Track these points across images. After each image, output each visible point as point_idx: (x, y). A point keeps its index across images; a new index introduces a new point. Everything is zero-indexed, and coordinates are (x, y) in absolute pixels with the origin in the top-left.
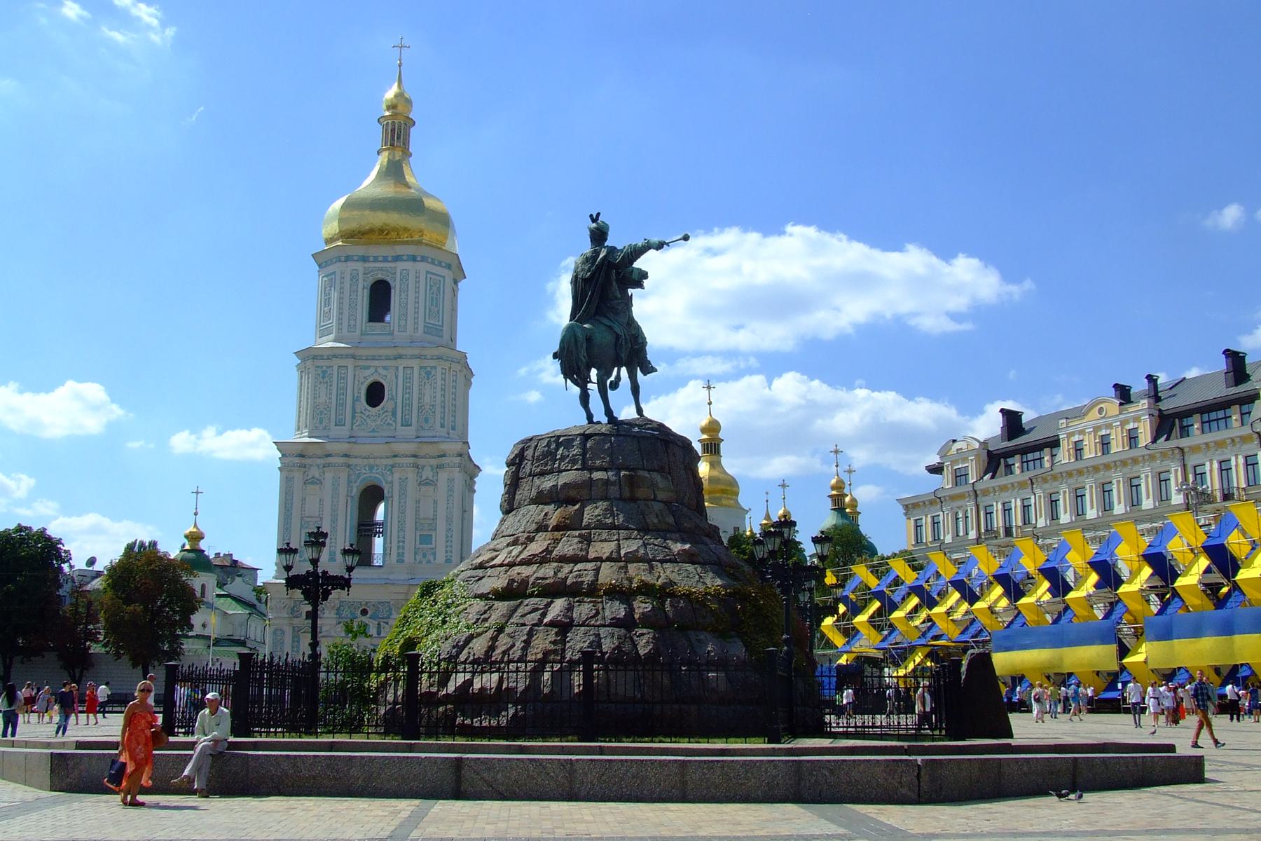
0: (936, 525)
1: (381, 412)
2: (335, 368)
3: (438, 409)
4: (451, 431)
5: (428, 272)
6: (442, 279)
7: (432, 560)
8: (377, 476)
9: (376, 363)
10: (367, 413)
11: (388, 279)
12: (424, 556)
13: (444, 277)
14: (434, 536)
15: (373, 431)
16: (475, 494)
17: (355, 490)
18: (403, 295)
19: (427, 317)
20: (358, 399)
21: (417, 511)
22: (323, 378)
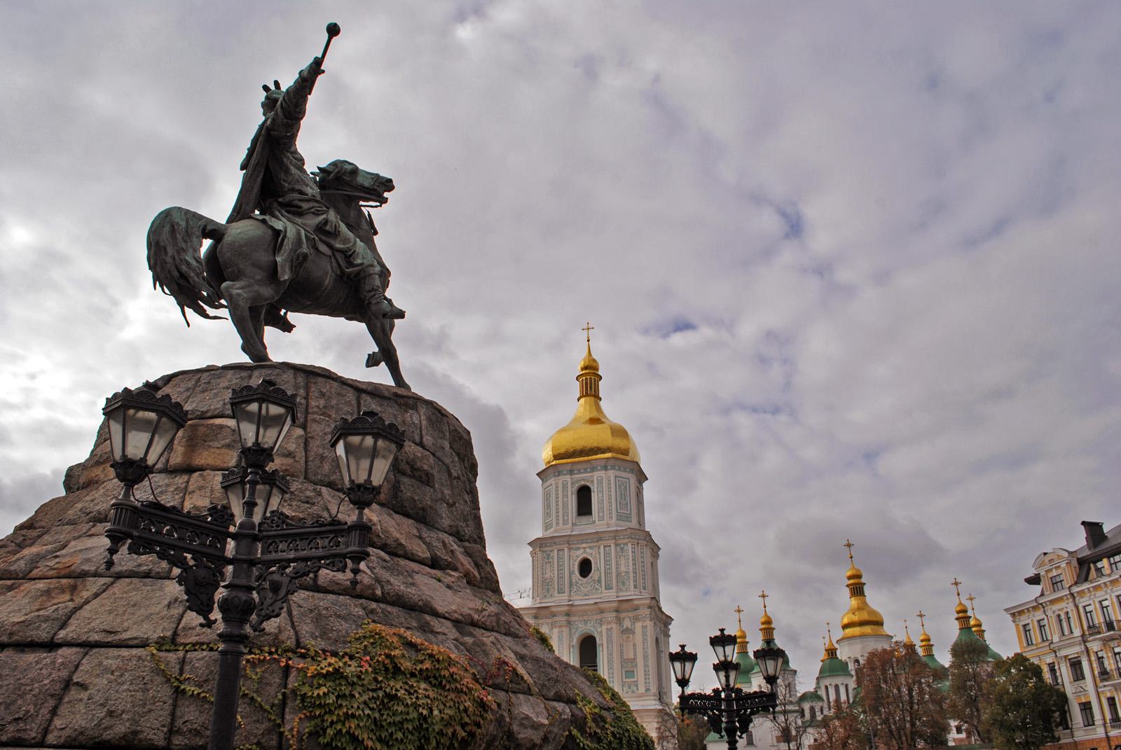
0: (1042, 628)
1: (590, 580)
2: (556, 552)
3: (631, 575)
4: (642, 591)
5: (616, 477)
6: (627, 480)
7: (636, 690)
8: (593, 629)
9: (584, 545)
10: (580, 582)
11: (589, 484)
12: (629, 687)
13: (629, 479)
14: (635, 672)
15: (586, 595)
16: (670, 639)
17: (575, 641)
18: (600, 495)
19: (619, 508)
20: (573, 573)
21: (622, 653)
22: (548, 559)
